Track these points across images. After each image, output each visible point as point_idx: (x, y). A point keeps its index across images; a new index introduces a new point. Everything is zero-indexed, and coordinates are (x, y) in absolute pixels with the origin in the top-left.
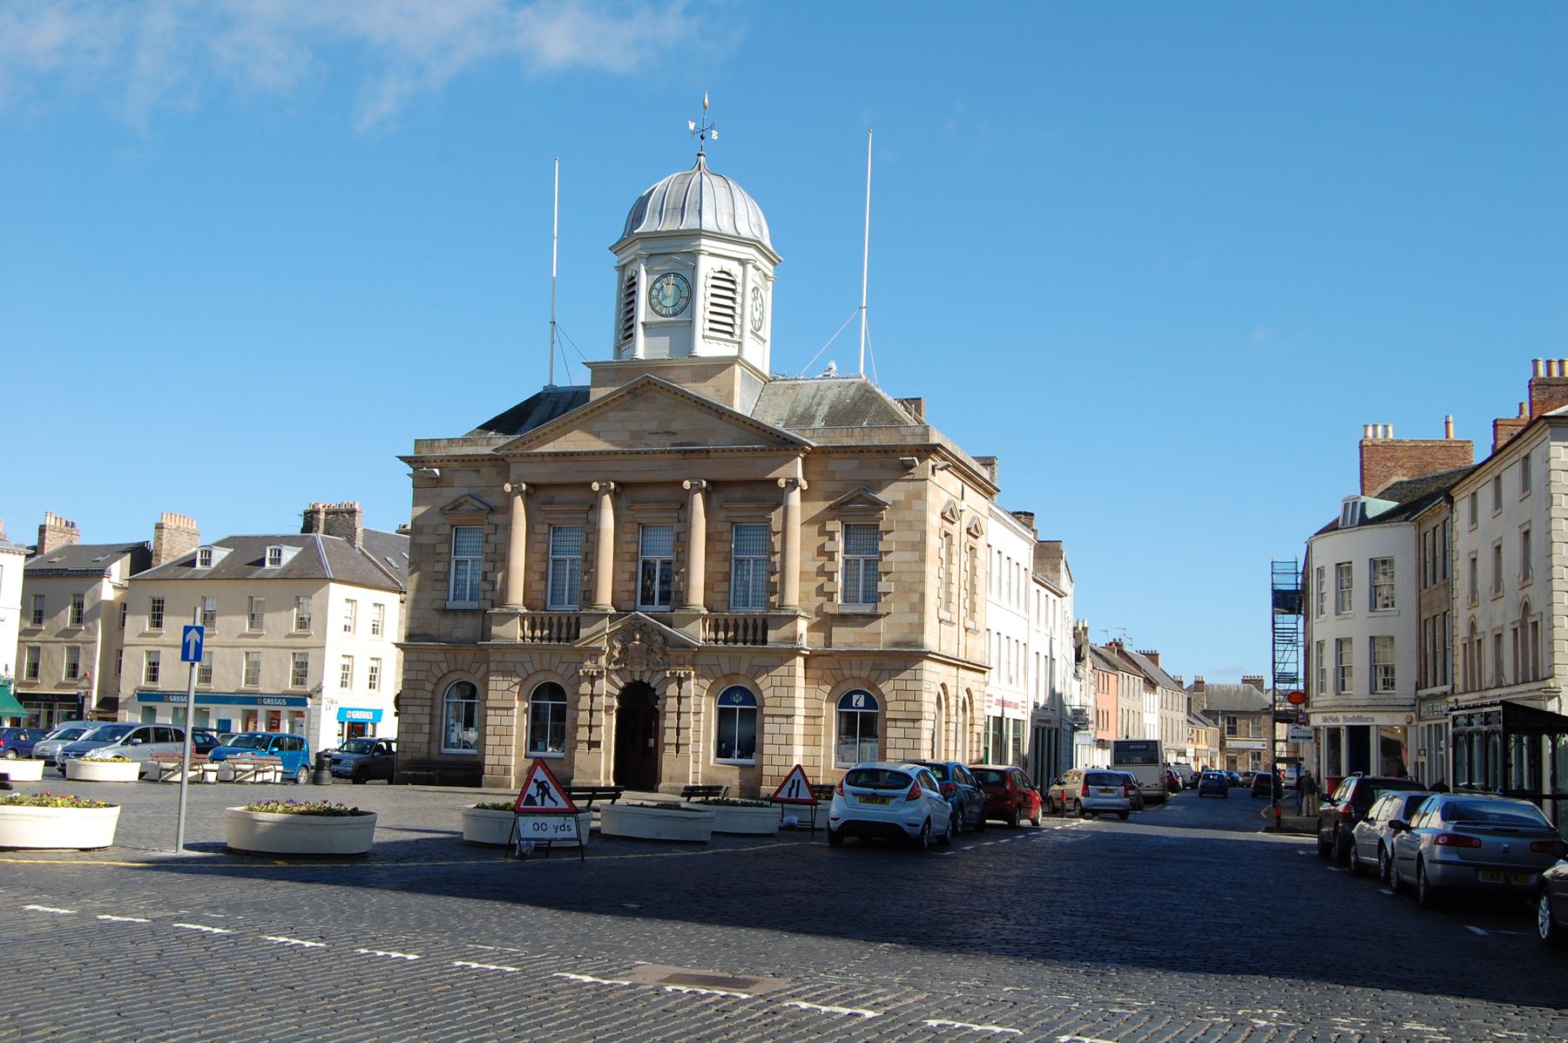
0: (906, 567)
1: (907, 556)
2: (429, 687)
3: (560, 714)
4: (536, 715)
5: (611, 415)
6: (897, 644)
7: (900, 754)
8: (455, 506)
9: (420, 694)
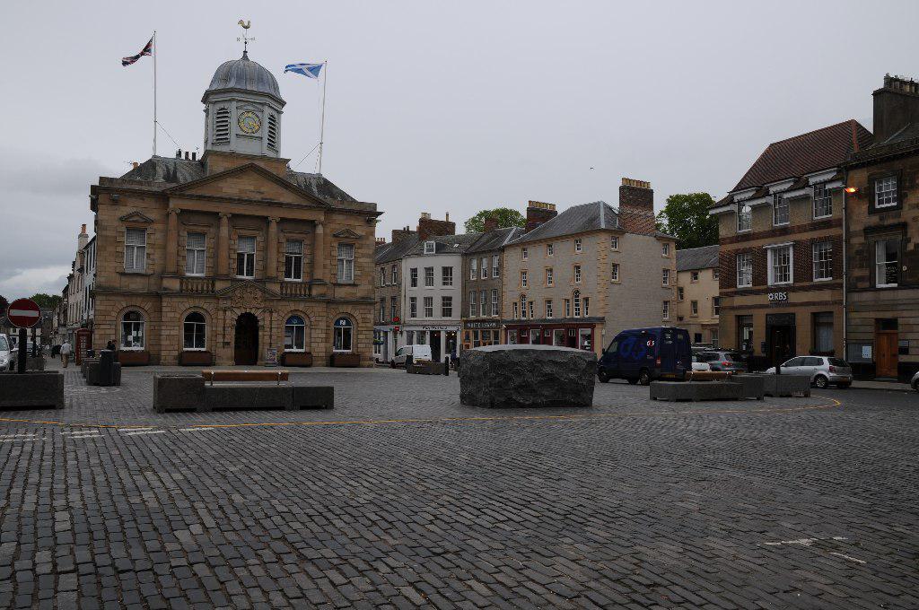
0: (365, 265)
1: (368, 260)
2: (114, 314)
3: (201, 329)
4: (188, 329)
5: (228, 179)
6: (363, 298)
8: (131, 215)
9: (108, 318)
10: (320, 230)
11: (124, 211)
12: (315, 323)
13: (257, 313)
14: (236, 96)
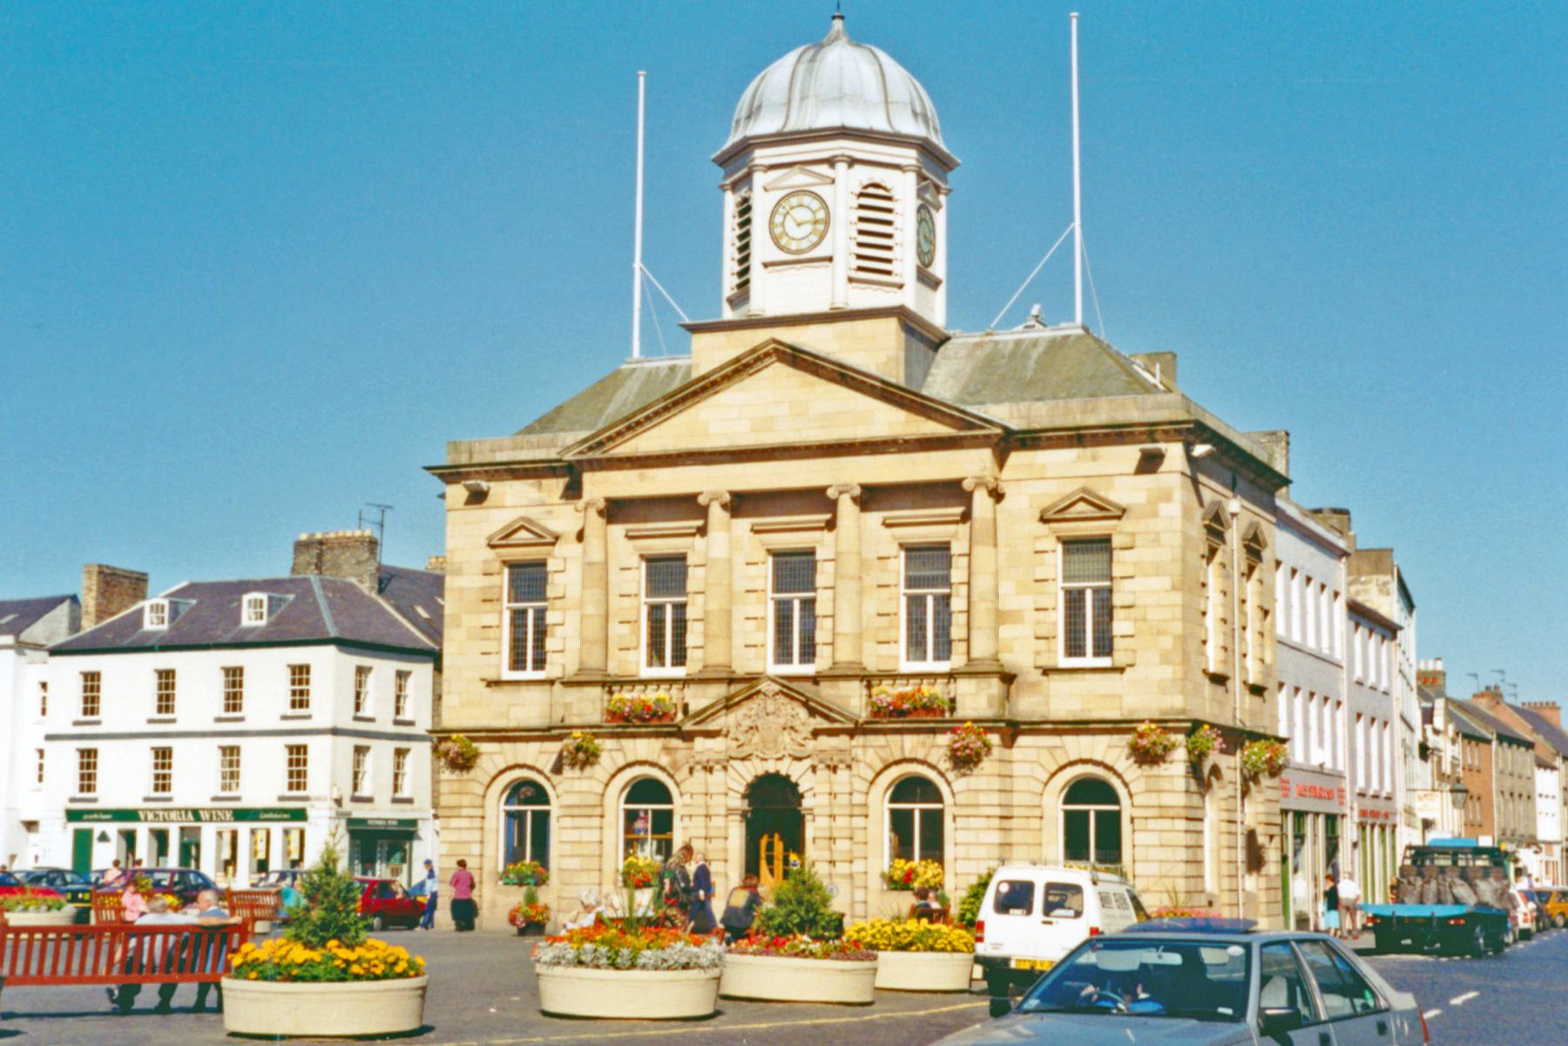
7: (1153, 869)
9: (465, 800)
10: (981, 501)
11: (492, 519)
12: (971, 799)
13: (796, 772)
14: (762, 156)
